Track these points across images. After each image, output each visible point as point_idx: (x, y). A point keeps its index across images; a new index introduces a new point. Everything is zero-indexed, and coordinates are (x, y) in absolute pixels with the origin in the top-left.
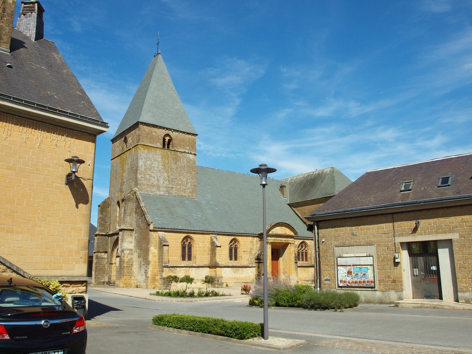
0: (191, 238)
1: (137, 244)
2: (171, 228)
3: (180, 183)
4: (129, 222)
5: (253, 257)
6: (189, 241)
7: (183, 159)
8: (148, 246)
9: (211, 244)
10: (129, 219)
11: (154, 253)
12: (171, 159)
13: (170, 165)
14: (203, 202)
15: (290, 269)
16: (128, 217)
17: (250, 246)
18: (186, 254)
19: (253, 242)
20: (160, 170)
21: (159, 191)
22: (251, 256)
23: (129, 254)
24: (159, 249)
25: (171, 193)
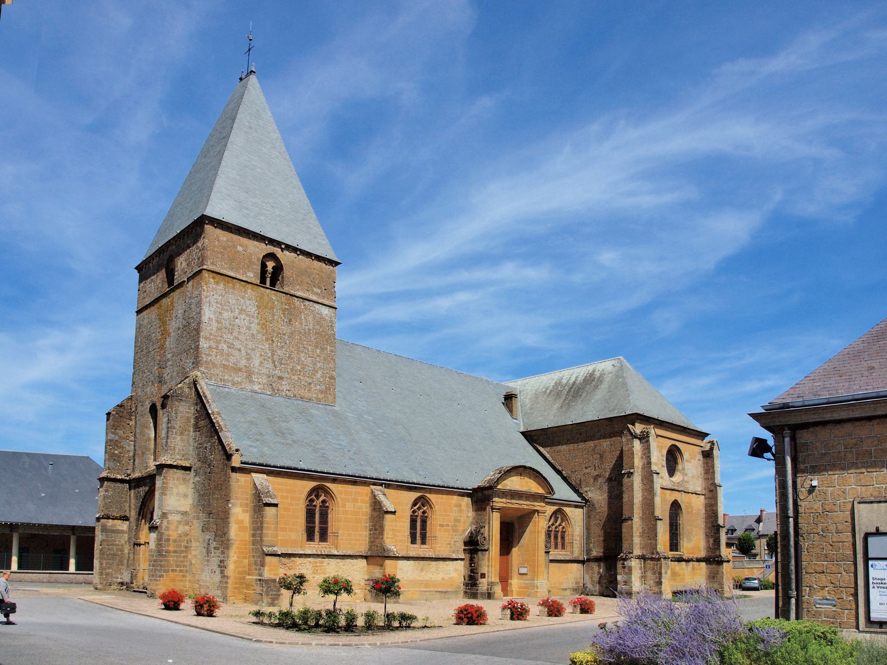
0: (327, 492)
1: (199, 500)
2: (282, 464)
3: (299, 368)
4: (179, 450)
5: (459, 539)
6: (321, 499)
7: (307, 315)
8: (227, 503)
9: (371, 506)
10: (180, 443)
11: (242, 521)
12: (278, 313)
13: (276, 325)
14: (349, 415)
15: (535, 565)
16: (178, 438)
17: (454, 514)
18: (314, 527)
19: (460, 506)
20: (253, 335)
21: (251, 382)
22: (456, 535)
23: (180, 522)
24: (255, 512)
25: (278, 390)
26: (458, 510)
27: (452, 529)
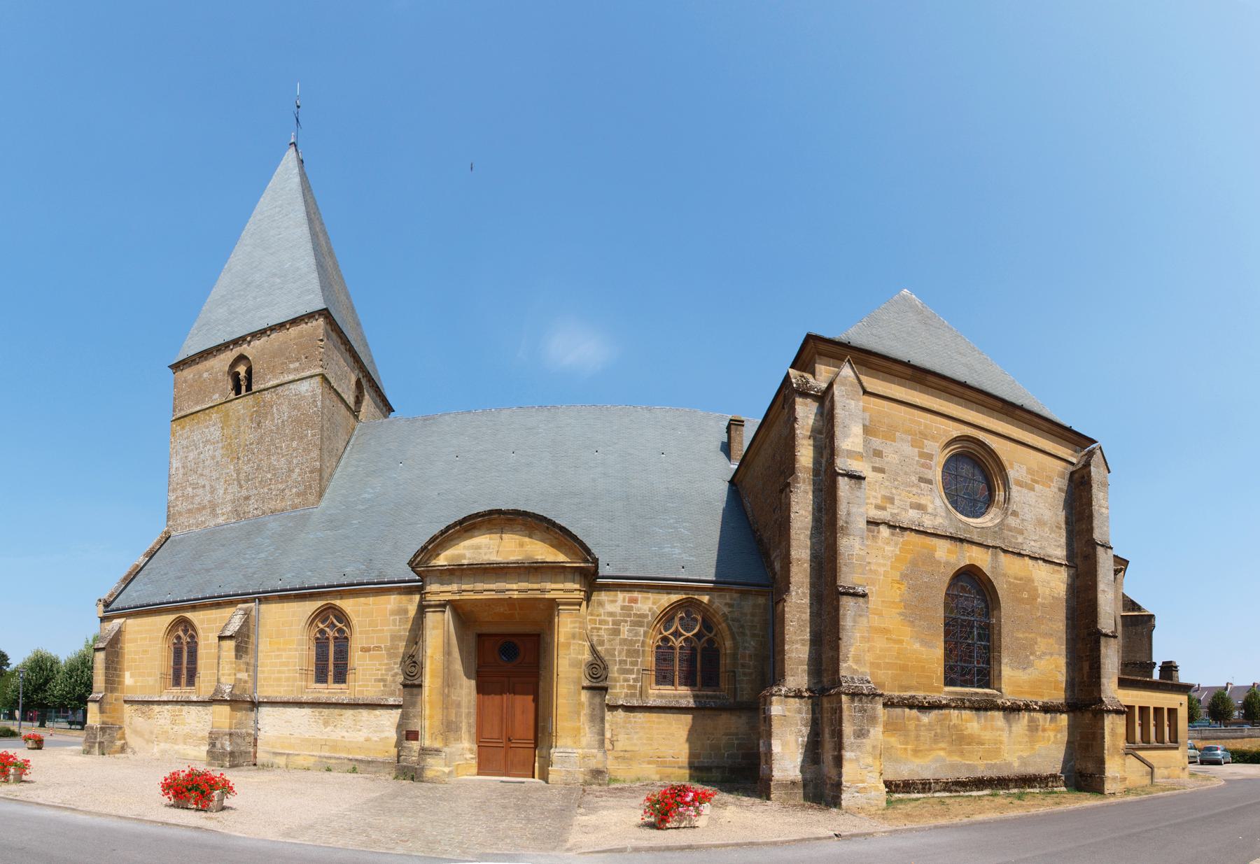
17: (391, 627)
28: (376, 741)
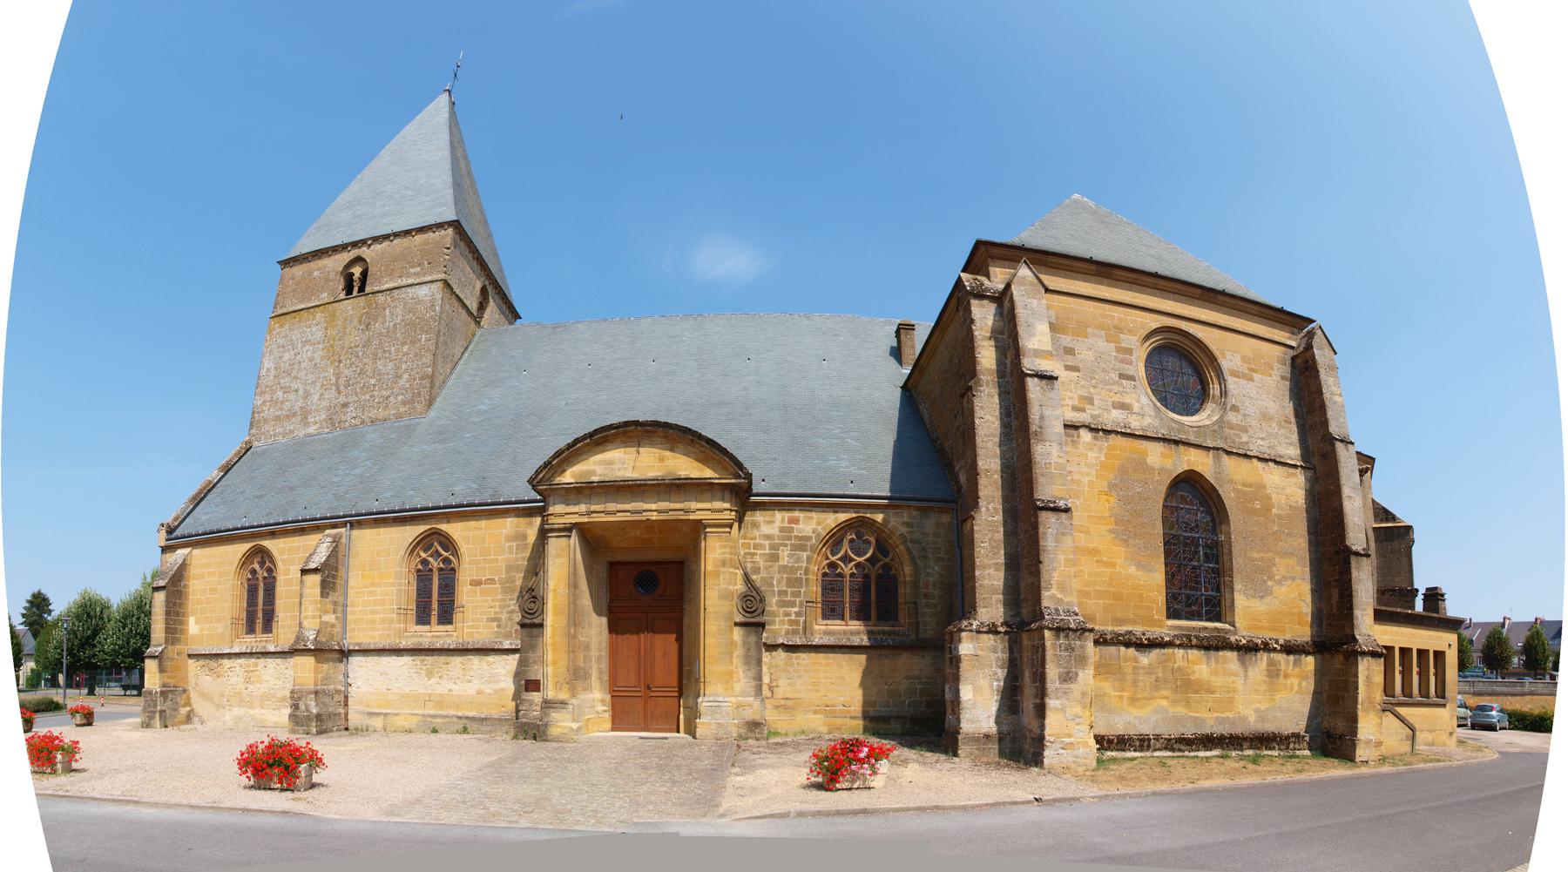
17: (507, 556)
26: (518, 545)
27: (502, 588)
28: (490, 694)
